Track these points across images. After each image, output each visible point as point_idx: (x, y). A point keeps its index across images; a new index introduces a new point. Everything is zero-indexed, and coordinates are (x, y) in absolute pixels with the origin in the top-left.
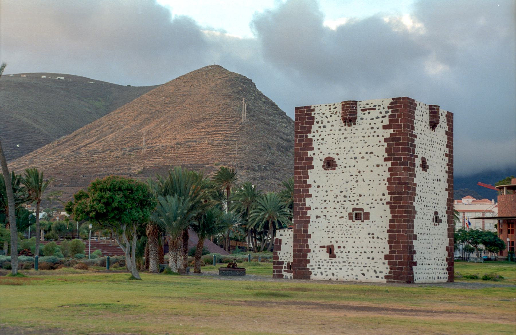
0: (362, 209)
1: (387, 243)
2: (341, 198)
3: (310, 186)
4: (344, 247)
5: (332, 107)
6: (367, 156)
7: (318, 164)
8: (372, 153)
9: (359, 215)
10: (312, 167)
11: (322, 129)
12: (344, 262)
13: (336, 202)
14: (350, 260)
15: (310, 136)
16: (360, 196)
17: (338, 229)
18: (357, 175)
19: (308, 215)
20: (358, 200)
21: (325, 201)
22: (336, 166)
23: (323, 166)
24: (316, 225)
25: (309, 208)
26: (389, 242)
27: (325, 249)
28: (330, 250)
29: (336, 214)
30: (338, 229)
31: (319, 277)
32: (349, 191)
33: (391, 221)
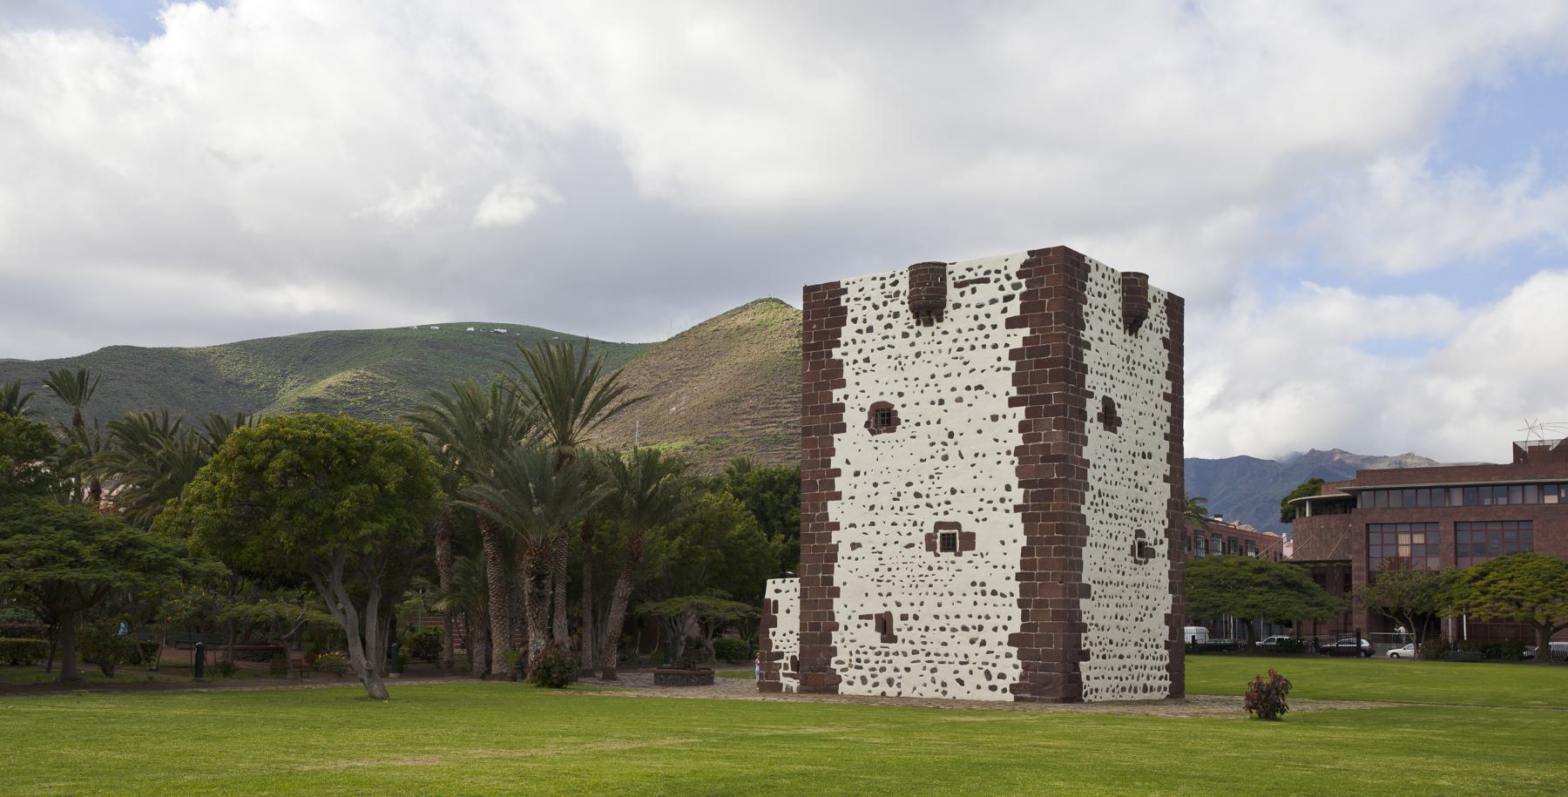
0: (957, 525)
1: (1015, 604)
2: (908, 499)
3: (838, 472)
4: (916, 617)
5: (889, 281)
6: (968, 396)
7: (855, 418)
8: (980, 387)
9: (951, 540)
10: (842, 428)
11: (865, 335)
12: (915, 652)
13: (897, 509)
14: (928, 648)
15: (836, 353)
16: (953, 491)
17: (902, 574)
18: (945, 444)
19: (834, 542)
20: (948, 503)
21: (872, 508)
22: (898, 422)
23: (867, 425)
24: (853, 564)
25: (836, 526)
26: (1021, 603)
27: (872, 623)
28: (884, 625)
29: (897, 537)
30: (902, 574)
31: (858, 689)
32: (928, 482)
33: (1025, 551)
